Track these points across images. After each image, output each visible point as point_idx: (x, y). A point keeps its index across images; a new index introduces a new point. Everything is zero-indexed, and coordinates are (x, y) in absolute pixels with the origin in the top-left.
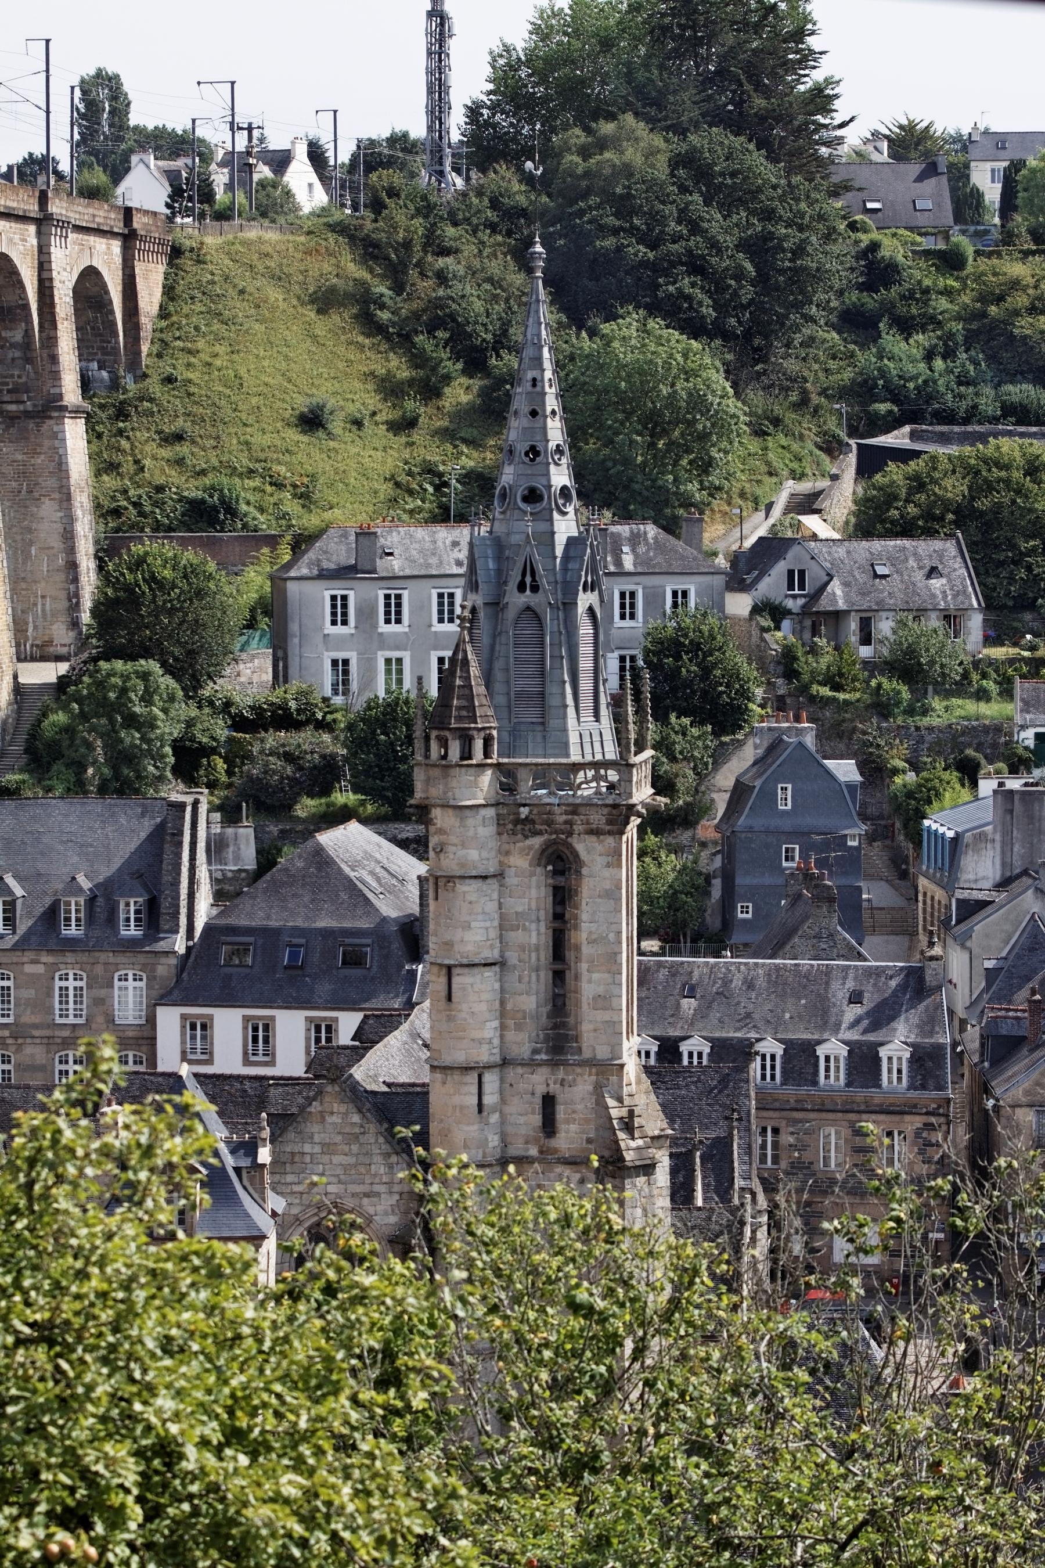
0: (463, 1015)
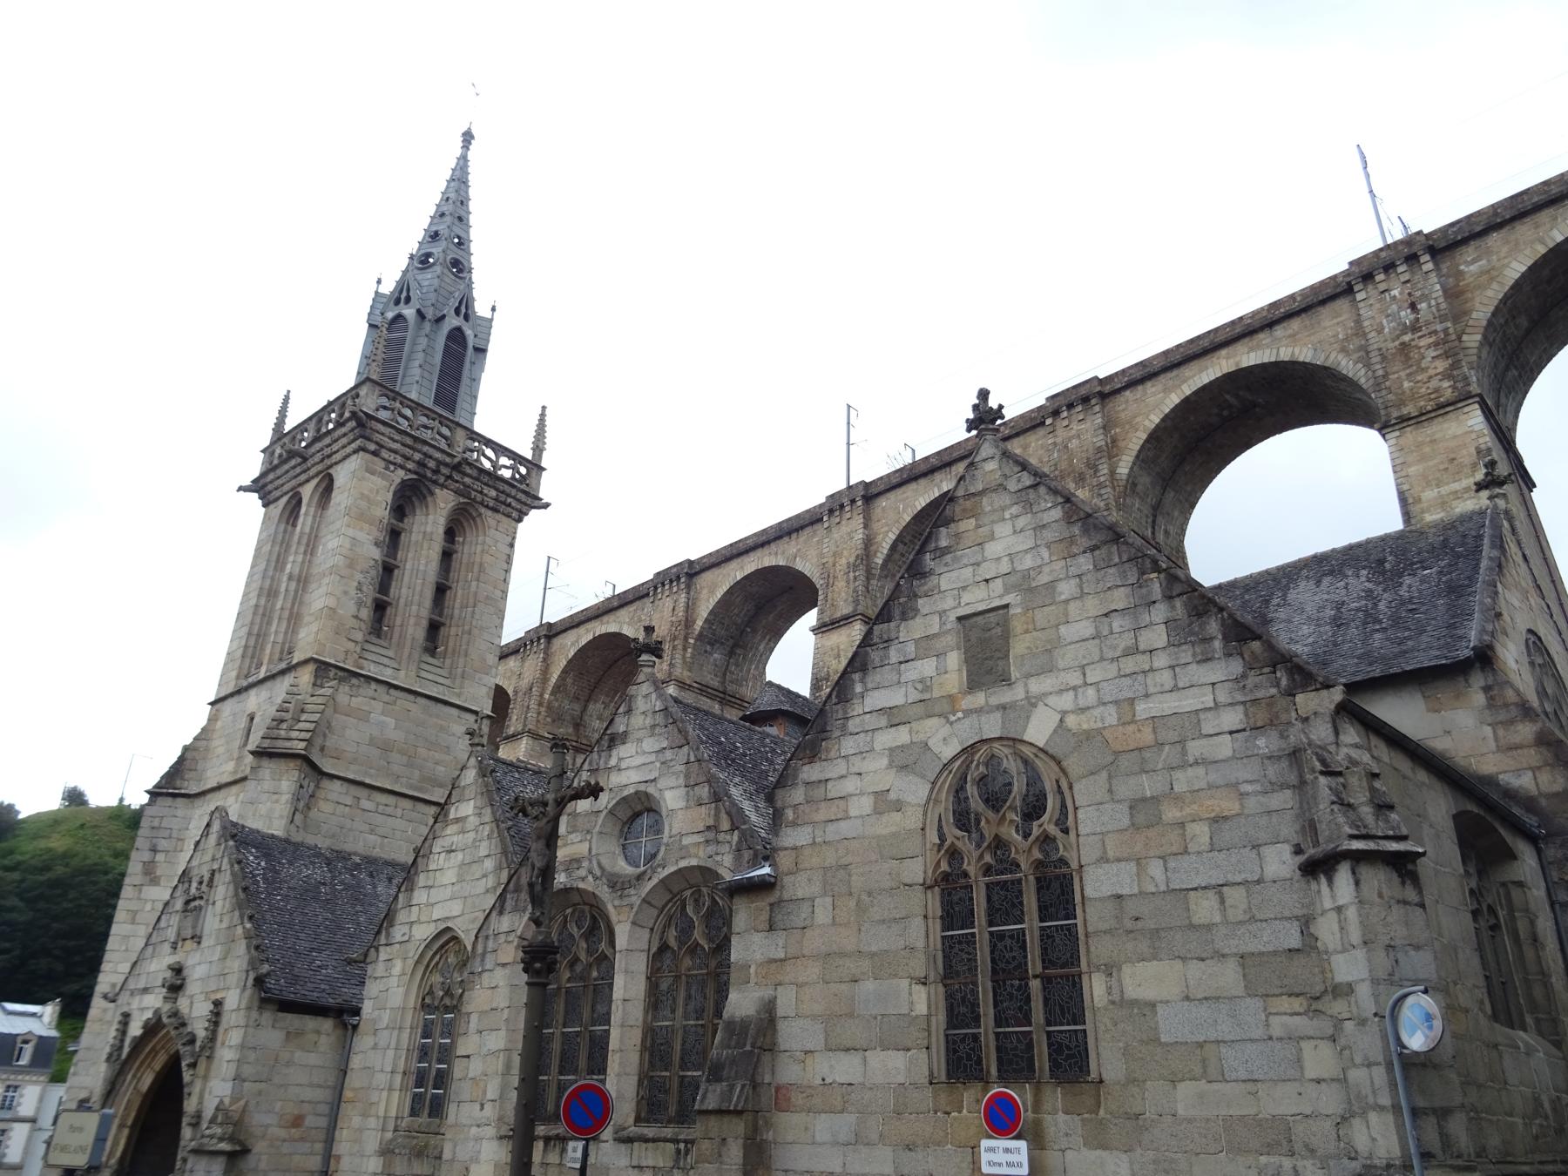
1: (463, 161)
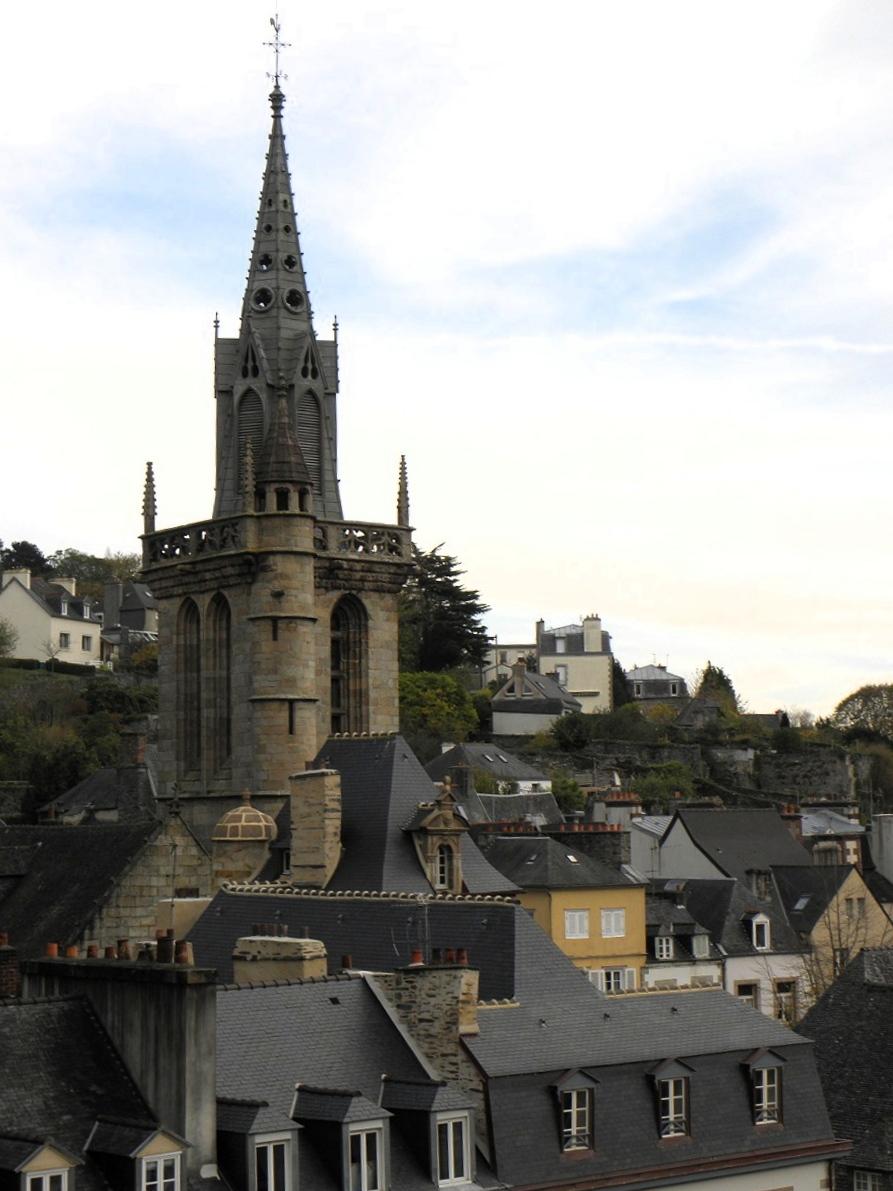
0: (304, 747)
1: (277, 137)
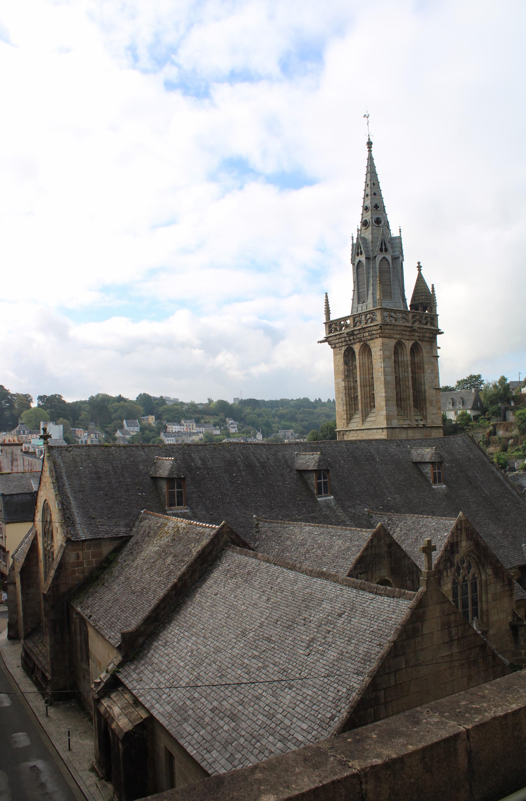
1: (370, 159)
